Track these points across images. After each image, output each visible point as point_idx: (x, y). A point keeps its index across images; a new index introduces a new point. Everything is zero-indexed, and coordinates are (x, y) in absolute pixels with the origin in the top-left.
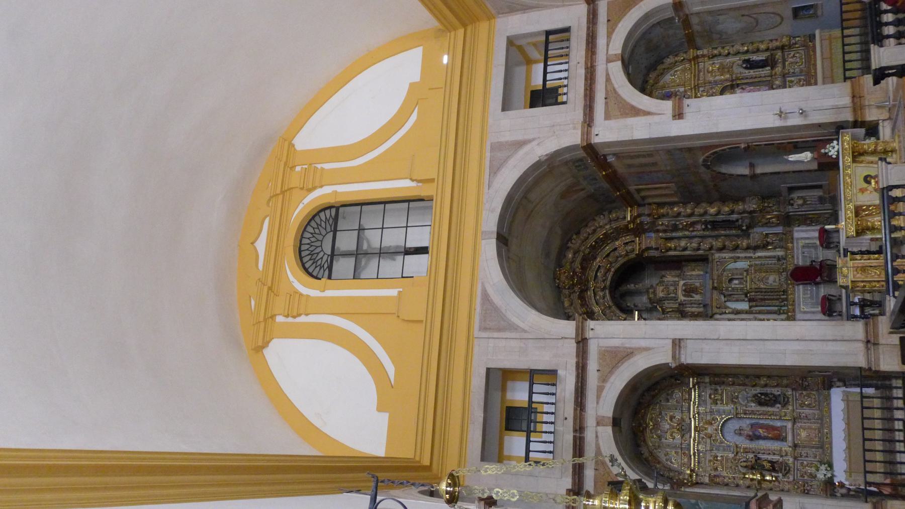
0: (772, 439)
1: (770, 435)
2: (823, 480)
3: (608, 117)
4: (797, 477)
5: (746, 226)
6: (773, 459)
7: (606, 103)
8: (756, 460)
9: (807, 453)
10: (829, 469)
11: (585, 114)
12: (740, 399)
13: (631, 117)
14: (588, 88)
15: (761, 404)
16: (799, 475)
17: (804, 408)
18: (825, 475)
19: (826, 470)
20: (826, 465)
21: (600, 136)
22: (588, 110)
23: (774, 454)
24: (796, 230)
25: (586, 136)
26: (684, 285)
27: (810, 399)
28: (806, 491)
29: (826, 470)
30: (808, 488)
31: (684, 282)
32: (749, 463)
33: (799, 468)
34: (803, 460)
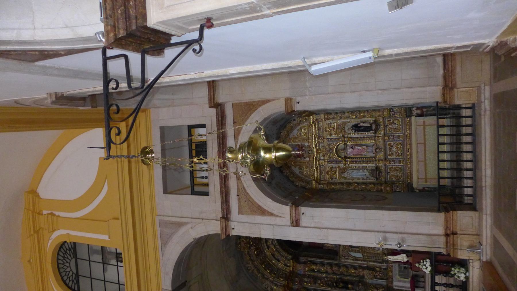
3: (241, 212)
7: (239, 199)
11: (223, 209)
13: (259, 215)
14: (223, 186)
21: (236, 230)
22: (225, 205)
25: (224, 230)
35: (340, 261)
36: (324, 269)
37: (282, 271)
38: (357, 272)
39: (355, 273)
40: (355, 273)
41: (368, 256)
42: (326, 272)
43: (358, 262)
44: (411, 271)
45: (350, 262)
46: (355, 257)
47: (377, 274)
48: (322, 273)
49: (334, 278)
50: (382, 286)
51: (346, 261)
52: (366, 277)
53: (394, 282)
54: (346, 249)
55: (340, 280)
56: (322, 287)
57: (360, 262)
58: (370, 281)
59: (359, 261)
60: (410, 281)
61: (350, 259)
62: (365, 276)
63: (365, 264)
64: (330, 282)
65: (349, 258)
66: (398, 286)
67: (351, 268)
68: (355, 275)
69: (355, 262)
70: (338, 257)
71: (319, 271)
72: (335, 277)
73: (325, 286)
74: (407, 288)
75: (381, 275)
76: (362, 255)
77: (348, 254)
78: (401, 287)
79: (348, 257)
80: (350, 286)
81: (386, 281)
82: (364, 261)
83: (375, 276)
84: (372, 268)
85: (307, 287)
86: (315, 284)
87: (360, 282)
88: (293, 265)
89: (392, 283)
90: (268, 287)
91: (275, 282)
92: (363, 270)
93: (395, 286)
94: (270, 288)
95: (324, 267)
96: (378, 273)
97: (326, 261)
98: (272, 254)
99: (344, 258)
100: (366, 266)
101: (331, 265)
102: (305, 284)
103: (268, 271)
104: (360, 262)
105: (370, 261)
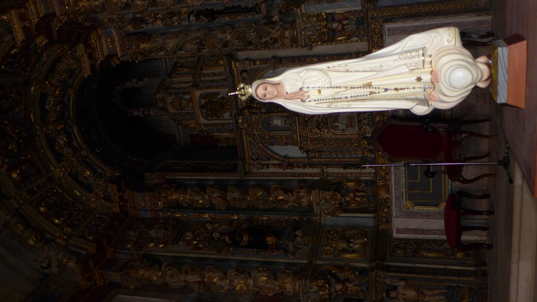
5: (280, 13)
24: (389, 30)
26: (202, 96)
31: (201, 92)
35: (247, 173)
36: (203, 199)
37: (97, 216)
38: (293, 198)
39: (287, 202)
40: (287, 202)
41: (319, 152)
42: (212, 208)
43: (296, 170)
44: (448, 181)
45: (274, 174)
46: (286, 157)
47: (348, 199)
48: (202, 209)
49: (231, 222)
50: (362, 231)
51: (263, 171)
52: (317, 210)
53: (394, 219)
54: (254, 135)
55: (244, 226)
56: (193, 249)
57: (301, 170)
58: (328, 220)
59: (299, 167)
60: (446, 209)
61: (274, 165)
62: (315, 207)
63: (315, 175)
64: (216, 235)
65: (271, 162)
66: (407, 231)
67: (276, 189)
68: (286, 207)
69: (287, 171)
70: (240, 163)
71: (192, 207)
72: (236, 217)
73: (201, 246)
74: (435, 234)
75: (358, 199)
76: (301, 148)
77: (264, 151)
78: (415, 231)
79: (269, 160)
80: (270, 240)
81: (372, 215)
82: (312, 165)
83: (341, 204)
84: (333, 184)
85: (153, 253)
86: (177, 243)
87: (296, 226)
88: (121, 198)
89: (389, 221)
90: (49, 266)
91: (73, 249)
92: (309, 192)
93: (399, 231)
94: (58, 266)
95: (205, 193)
96: (352, 195)
97: (210, 177)
98: (70, 174)
99: (256, 162)
100: (318, 178)
101: (222, 186)
102: (152, 245)
103: (57, 221)
104: (301, 170)
105: (327, 165)
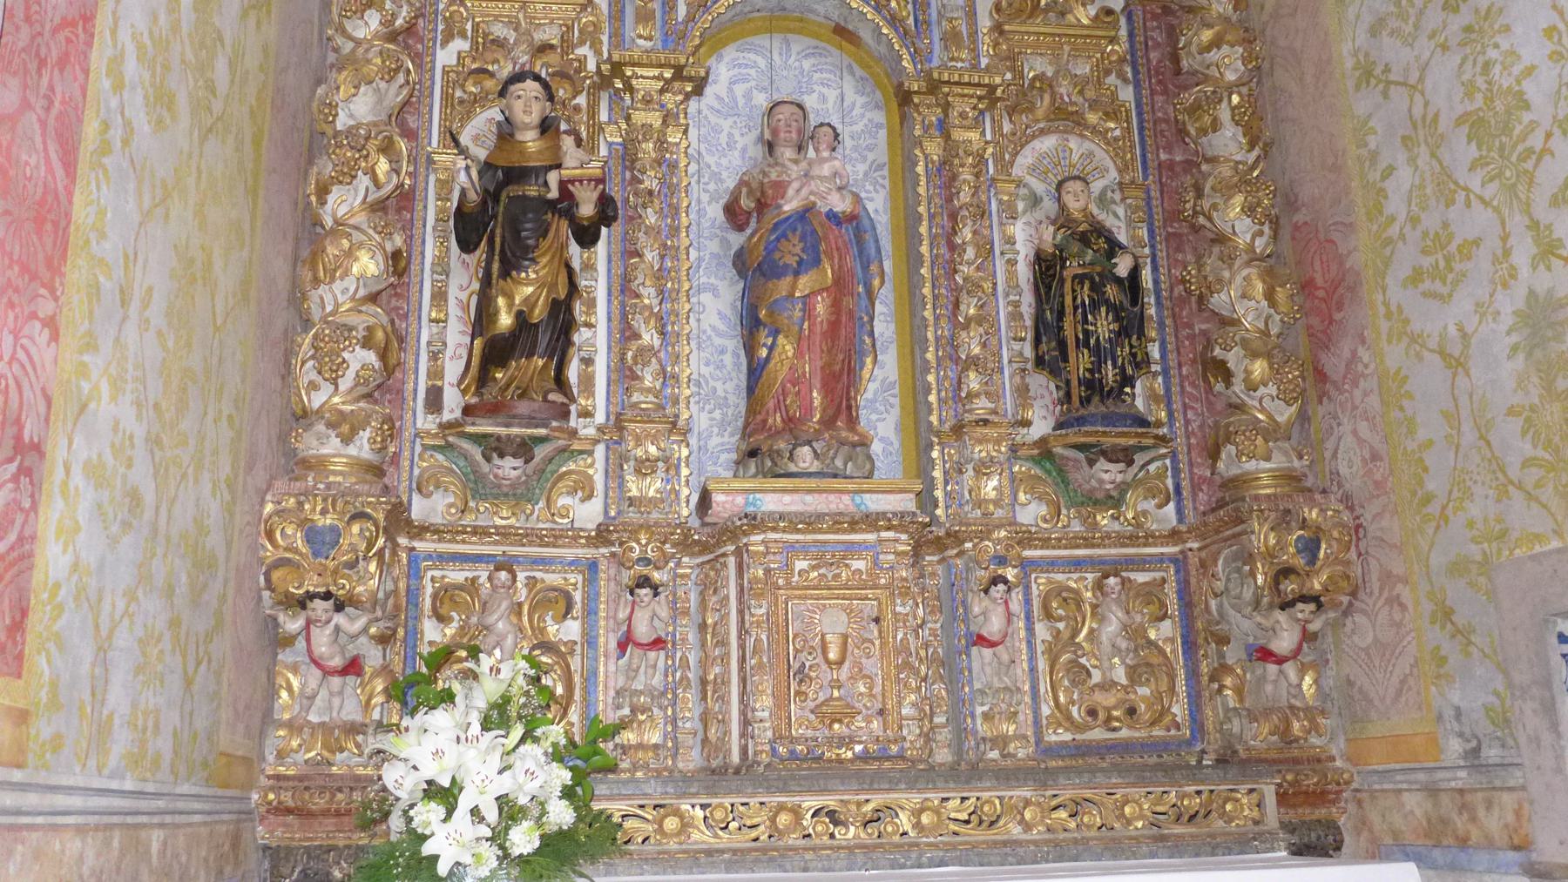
0: (755, 372)
1: (789, 348)
2: (391, 775)
4: (444, 559)
6: (588, 362)
8: (565, 203)
9: (658, 643)
10: (523, 840)
12: (1048, 143)
15: (1047, 268)
16: (457, 576)
17: (1042, 631)
18: (444, 795)
19: (510, 811)
20: (561, 814)
23: (624, 375)
27: (1120, 675)
28: (292, 624)
29: (510, 811)
30: (322, 641)
32: (530, 139)
33: (521, 576)
34: (590, 612)
